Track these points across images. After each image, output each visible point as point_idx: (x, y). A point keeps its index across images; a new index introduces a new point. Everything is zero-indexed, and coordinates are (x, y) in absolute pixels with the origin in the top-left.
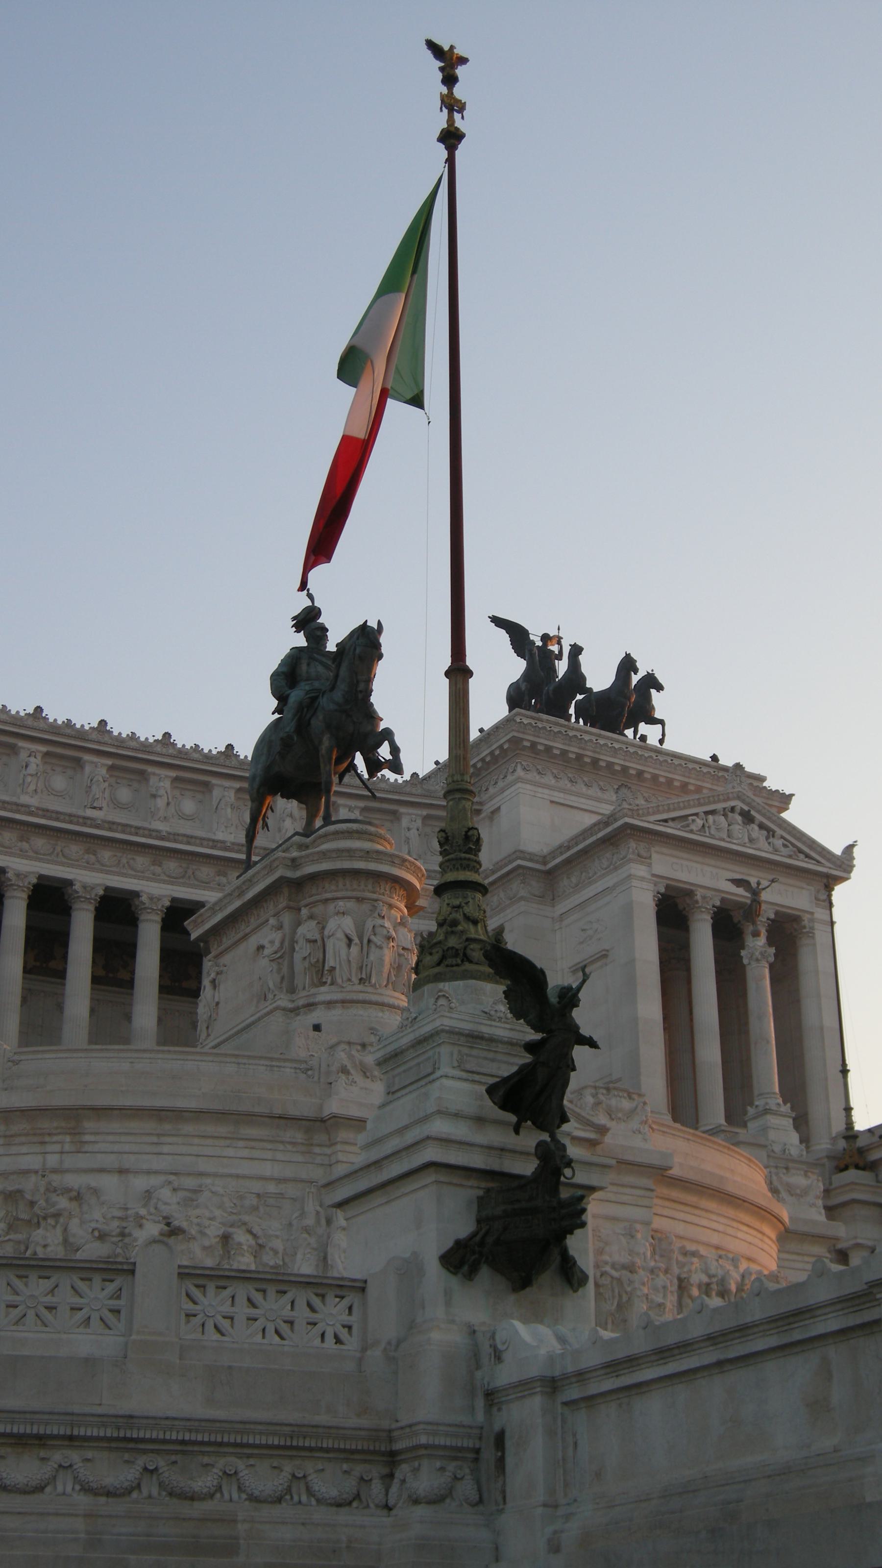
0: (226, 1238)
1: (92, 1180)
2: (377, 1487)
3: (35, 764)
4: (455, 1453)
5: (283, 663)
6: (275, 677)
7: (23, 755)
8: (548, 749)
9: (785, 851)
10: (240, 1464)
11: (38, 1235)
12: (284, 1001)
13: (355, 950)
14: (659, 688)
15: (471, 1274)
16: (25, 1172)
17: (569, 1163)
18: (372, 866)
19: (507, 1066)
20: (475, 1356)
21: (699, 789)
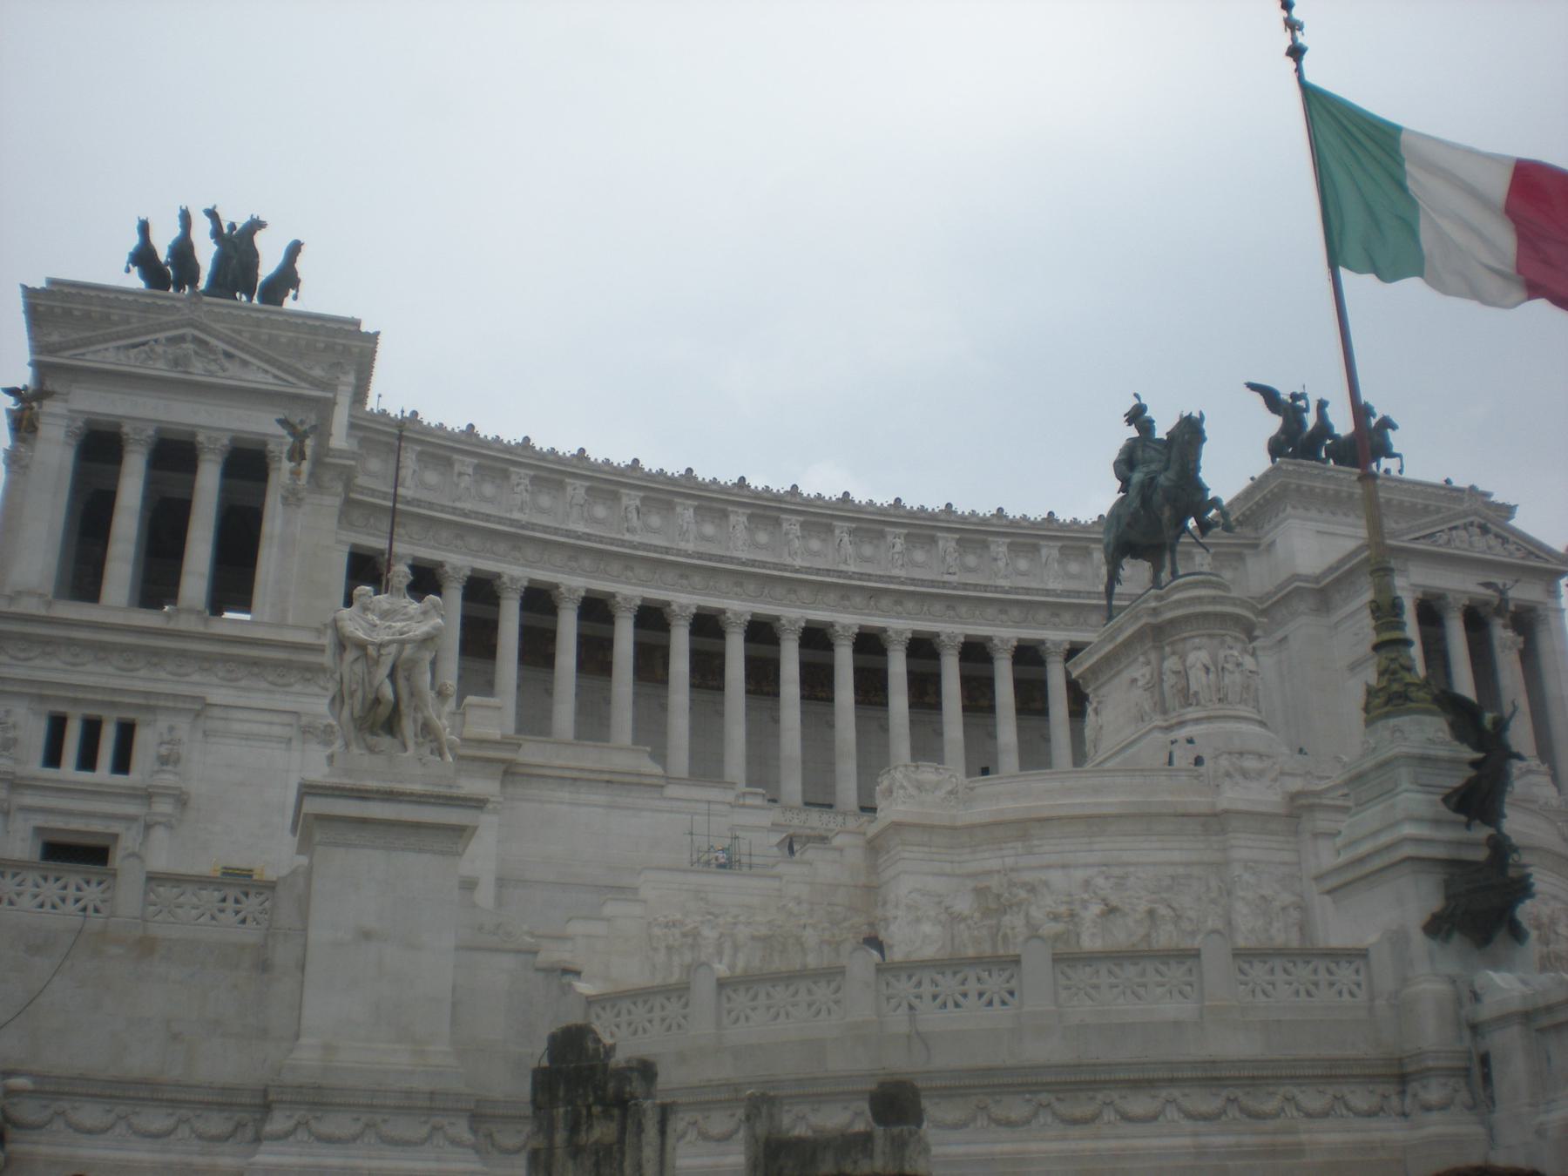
0: (1151, 913)
2: (1395, 1101)
3: (899, 545)
4: (1452, 1072)
5: (1122, 452)
6: (1117, 465)
7: (890, 538)
8: (1311, 489)
9: (1518, 554)
10: (1295, 1091)
11: (1006, 919)
12: (1159, 721)
13: (1212, 676)
14: (1394, 427)
15: (1447, 938)
16: (989, 873)
17: (1515, 849)
18: (1219, 608)
19: (1456, 780)
20: (1458, 1001)
21: (1438, 511)
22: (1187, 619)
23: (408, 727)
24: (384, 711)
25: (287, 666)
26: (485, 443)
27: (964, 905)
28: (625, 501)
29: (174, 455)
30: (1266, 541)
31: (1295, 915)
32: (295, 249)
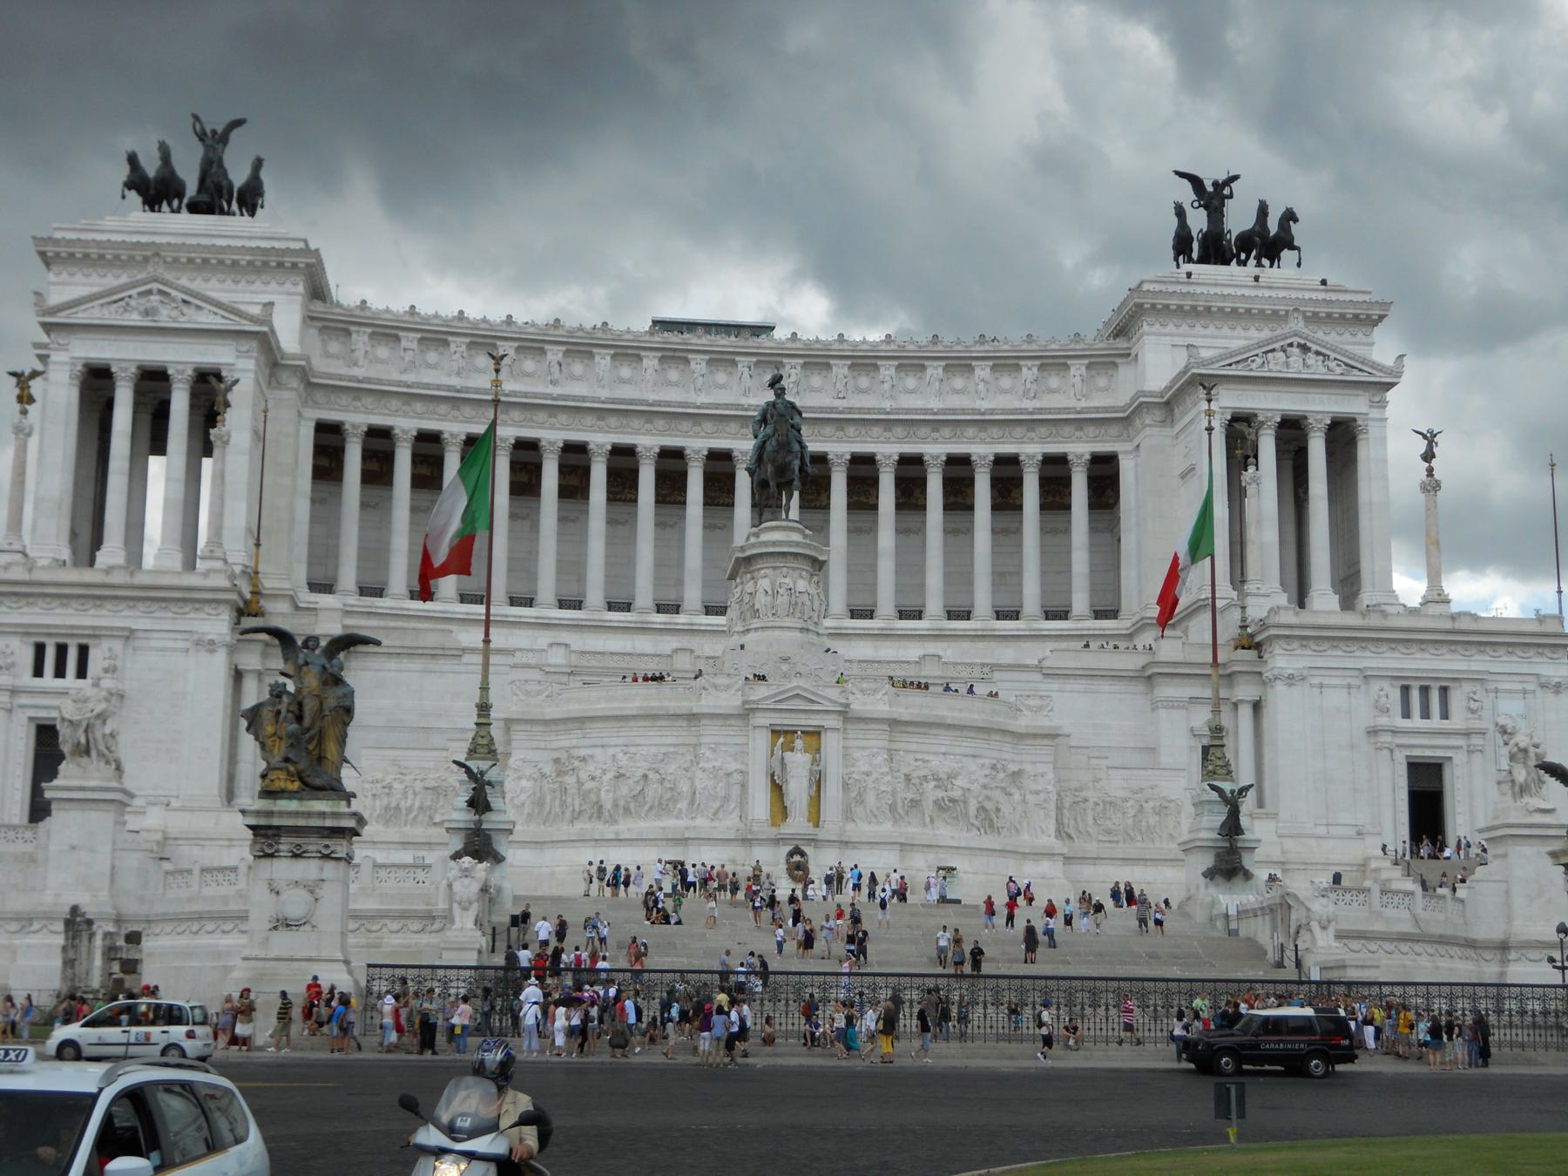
0: (645, 776)
1: (589, 751)
8: (1167, 307)
9: (1339, 370)
13: (769, 598)
14: (1296, 220)
22: (761, 555)
23: (93, 753)
24: (83, 748)
25: (184, 600)
26: (426, 320)
27: (548, 769)
28: (550, 356)
29: (153, 381)
30: (1133, 353)
31: (737, 777)
32: (258, 164)
